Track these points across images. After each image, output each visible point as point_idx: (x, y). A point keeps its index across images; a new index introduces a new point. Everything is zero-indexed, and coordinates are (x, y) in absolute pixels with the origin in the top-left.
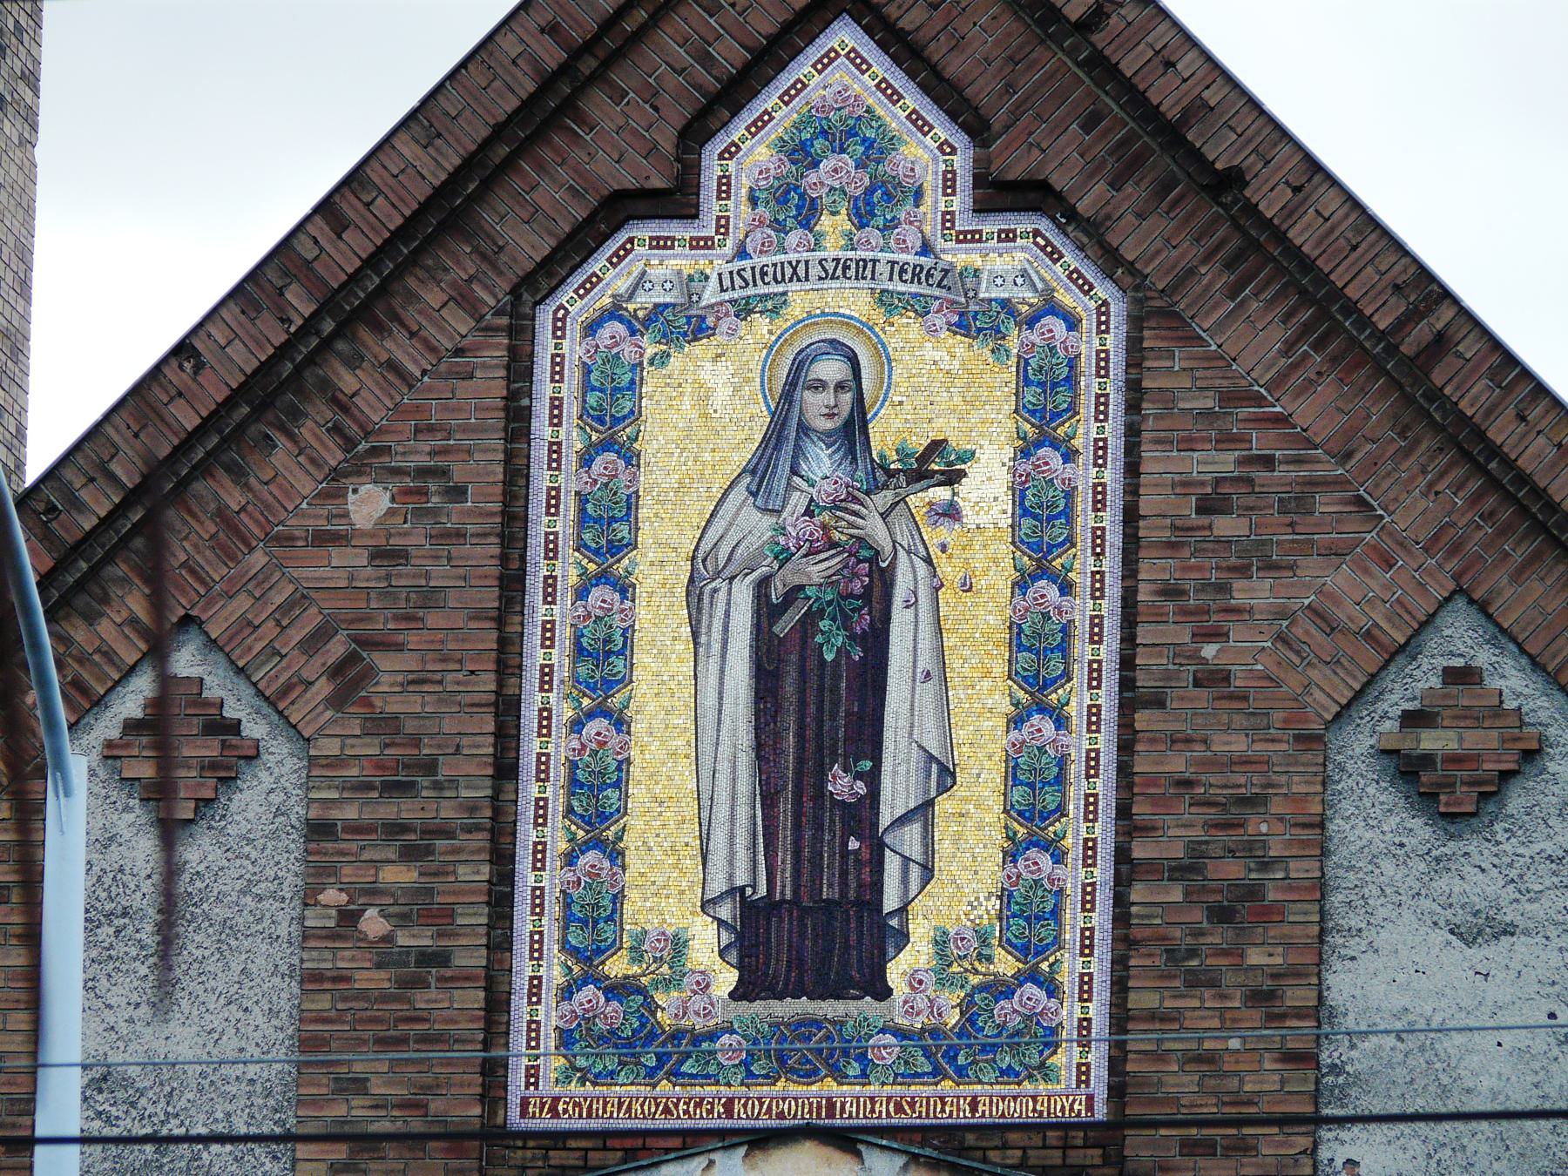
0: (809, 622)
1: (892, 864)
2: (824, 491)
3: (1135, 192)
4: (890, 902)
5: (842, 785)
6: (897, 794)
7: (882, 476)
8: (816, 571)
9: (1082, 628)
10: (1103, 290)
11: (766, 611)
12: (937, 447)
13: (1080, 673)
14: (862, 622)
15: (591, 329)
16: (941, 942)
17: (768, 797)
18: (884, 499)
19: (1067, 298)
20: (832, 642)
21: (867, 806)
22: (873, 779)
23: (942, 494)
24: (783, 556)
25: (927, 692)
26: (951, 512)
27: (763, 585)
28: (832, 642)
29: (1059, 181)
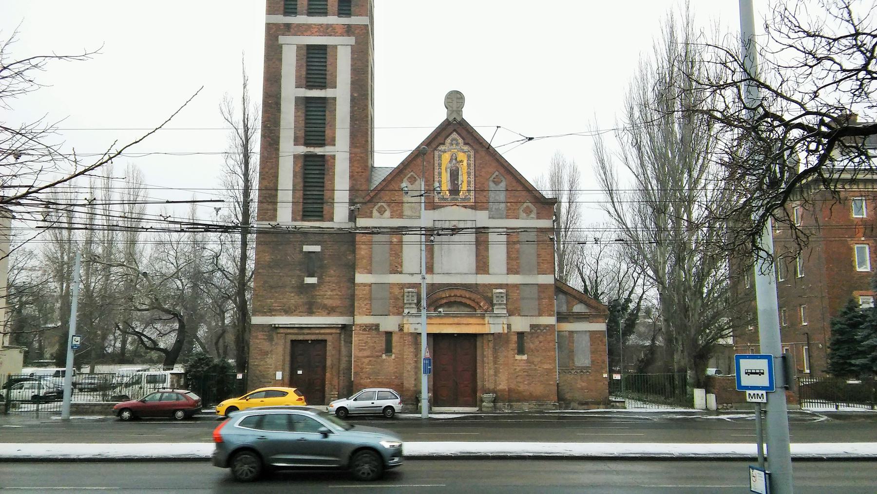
20: (455, 173)
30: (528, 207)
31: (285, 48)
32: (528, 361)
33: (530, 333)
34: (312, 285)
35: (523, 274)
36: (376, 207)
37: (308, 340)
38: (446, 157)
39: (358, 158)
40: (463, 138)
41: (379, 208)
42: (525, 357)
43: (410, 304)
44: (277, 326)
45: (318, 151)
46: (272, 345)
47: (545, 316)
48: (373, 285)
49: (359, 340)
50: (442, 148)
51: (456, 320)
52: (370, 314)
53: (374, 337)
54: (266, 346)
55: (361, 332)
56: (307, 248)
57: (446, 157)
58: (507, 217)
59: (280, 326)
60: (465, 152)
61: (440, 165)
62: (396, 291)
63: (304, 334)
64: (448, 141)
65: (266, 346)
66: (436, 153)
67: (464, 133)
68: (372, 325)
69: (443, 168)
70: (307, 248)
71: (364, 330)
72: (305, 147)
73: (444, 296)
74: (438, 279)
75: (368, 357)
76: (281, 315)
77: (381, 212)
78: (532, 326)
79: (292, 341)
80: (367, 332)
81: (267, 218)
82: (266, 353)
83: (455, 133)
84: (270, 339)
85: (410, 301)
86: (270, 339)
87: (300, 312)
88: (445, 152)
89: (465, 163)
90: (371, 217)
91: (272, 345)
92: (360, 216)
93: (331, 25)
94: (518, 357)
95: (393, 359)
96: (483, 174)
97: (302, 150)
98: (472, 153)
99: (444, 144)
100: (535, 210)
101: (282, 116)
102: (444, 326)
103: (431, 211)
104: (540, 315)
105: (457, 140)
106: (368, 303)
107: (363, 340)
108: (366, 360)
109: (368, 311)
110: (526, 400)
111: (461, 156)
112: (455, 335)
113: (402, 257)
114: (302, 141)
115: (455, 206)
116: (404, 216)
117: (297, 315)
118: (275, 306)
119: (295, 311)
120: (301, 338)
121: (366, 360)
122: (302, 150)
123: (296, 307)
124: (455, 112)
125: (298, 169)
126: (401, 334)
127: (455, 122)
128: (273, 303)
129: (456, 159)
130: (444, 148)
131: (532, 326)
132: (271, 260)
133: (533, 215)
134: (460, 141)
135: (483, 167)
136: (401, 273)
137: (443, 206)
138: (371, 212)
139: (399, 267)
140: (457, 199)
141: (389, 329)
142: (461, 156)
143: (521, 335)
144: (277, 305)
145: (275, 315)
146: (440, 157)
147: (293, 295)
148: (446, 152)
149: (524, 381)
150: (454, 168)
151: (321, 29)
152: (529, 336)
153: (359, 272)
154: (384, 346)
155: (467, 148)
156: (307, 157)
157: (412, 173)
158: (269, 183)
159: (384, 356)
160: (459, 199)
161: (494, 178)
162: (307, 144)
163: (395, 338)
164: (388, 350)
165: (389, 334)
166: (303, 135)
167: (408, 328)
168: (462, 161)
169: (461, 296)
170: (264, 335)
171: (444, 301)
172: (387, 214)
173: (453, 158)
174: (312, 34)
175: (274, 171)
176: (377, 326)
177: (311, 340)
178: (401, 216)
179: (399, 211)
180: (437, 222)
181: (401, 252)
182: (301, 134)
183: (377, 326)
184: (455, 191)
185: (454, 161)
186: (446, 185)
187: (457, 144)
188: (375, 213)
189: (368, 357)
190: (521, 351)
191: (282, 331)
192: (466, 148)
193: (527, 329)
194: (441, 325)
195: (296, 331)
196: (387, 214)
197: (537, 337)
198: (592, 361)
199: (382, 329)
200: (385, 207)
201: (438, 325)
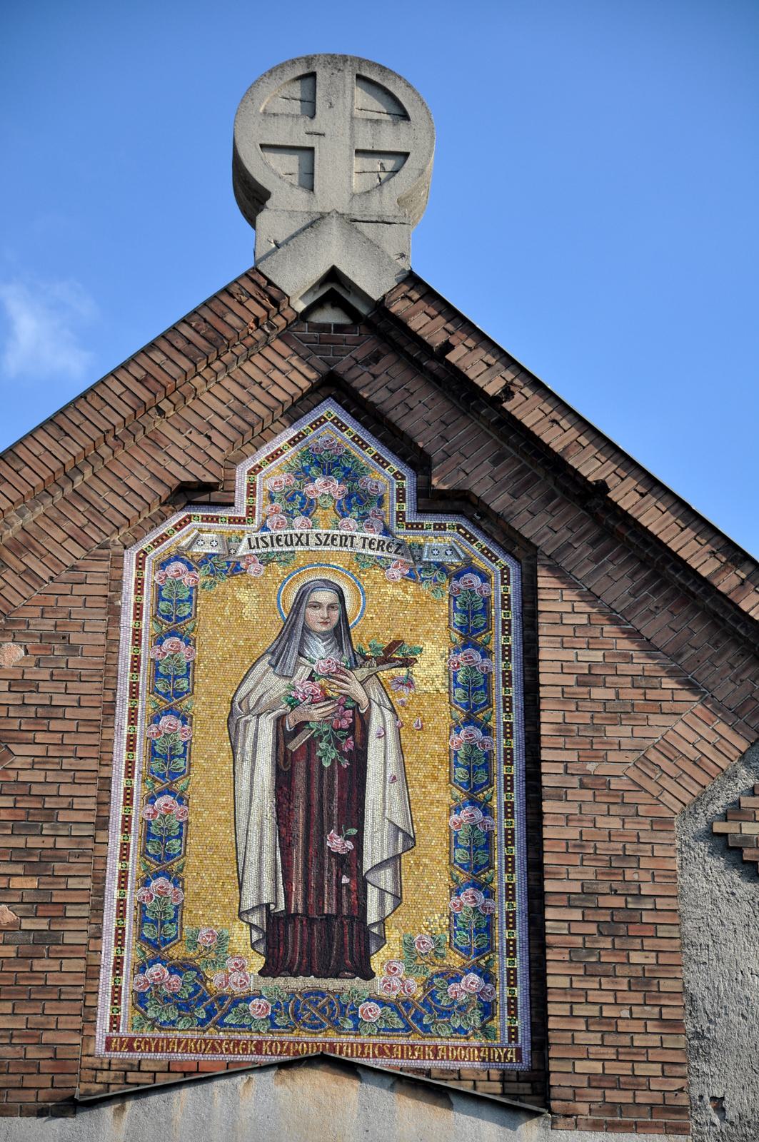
0: (311, 744)
1: (372, 894)
2: (321, 666)
3: (525, 502)
4: (372, 917)
5: (337, 843)
6: (375, 848)
7: (358, 659)
8: (316, 713)
9: (499, 755)
10: (504, 561)
11: (282, 735)
12: (396, 644)
13: (499, 783)
14: (348, 745)
15: (163, 565)
16: (408, 945)
17: (285, 845)
18: (361, 673)
19: (481, 563)
20: (327, 756)
21: (351, 861)
22: (358, 840)
23: (403, 672)
24: (294, 703)
25: (394, 790)
26: (408, 683)
27: (280, 720)
28: (327, 756)
29: (479, 491)
40: (419, 462)
83: (329, 409)
96: (616, 767)
105: (351, 474)
115: (316, 1082)
124: (333, 230)
127: (329, 316)
129: (340, 633)
135: (620, 712)
137: (196, 1077)
148: (236, 569)
155: (448, 539)
160: (372, 1012)
161: (735, 811)
185: (320, 651)
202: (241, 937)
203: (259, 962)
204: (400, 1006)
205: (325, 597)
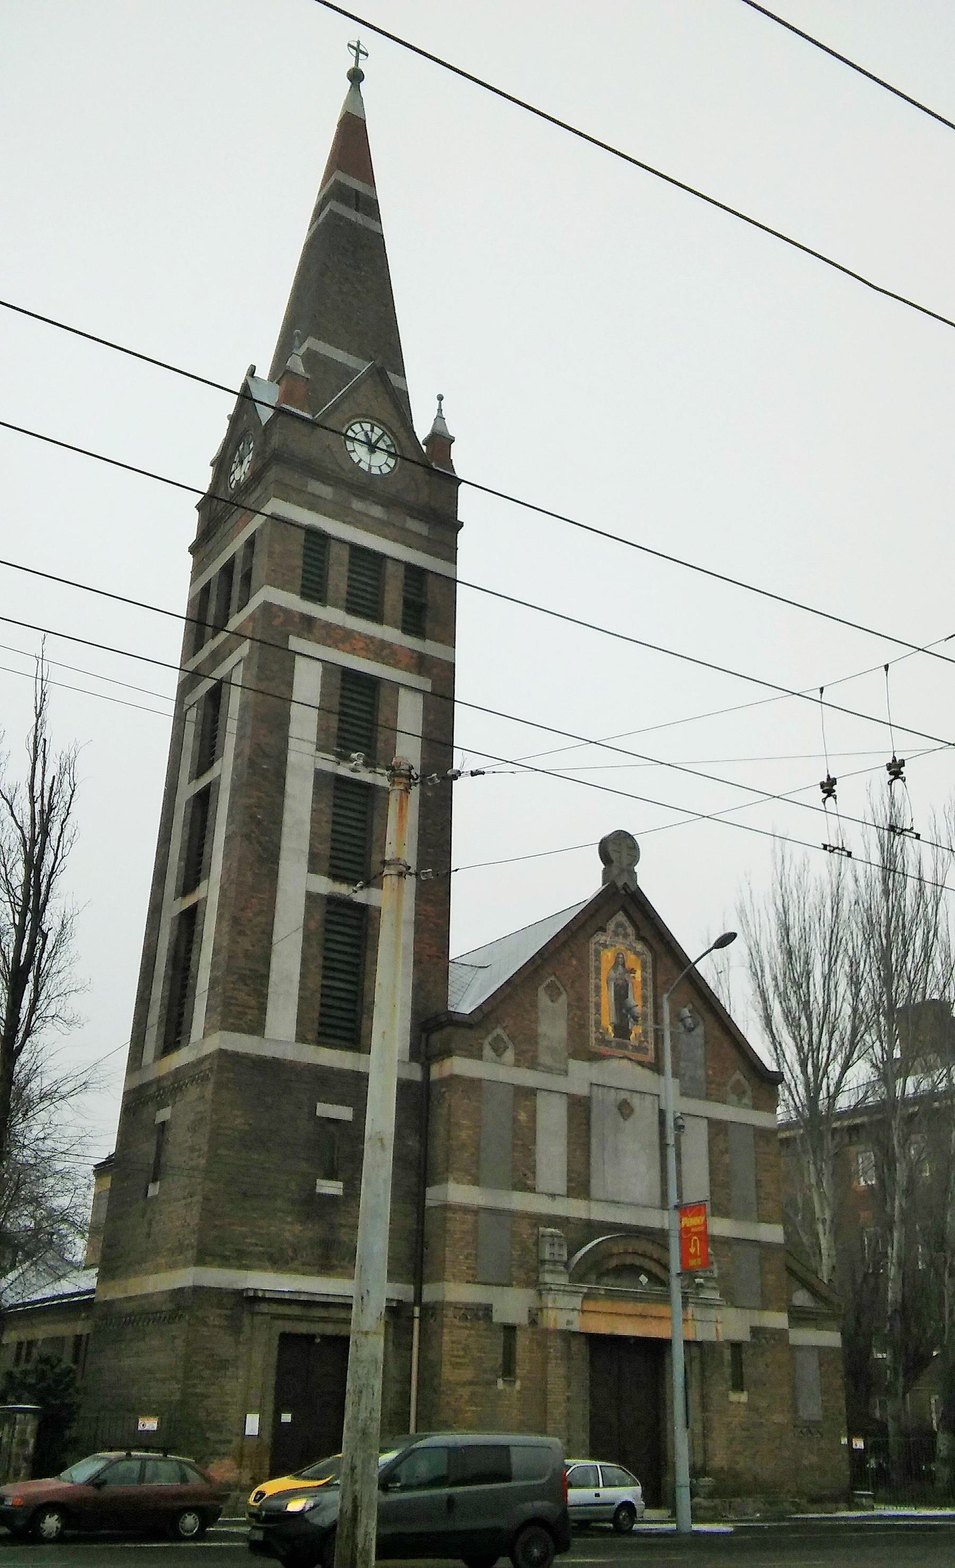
11: (616, 986)
23: (632, 975)
26: (634, 978)
30: (738, 1081)
31: (300, 662)
32: (750, 1406)
33: (753, 1346)
34: (332, 1199)
35: (737, 1219)
36: (490, 1038)
37: (313, 1337)
38: (608, 956)
39: (431, 925)
41: (495, 1039)
42: (743, 1397)
43: (555, 1262)
44: (260, 1294)
45: (360, 897)
46: (237, 1343)
47: (773, 1310)
48: (482, 1215)
49: (453, 1342)
50: (601, 938)
51: (640, 1307)
52: (473, 1280)
53: (481, 1336)
54: (224, 1346)
55: (457, 1322)
56: (325, 1110)
57: (608, 956)
58: (708, 1097)
59: (268, 1295)
60: (637, 954)
61: (598, 970)
62: (525, 1230)
63: (311, 1320)
64: (611, 926)
65: (224, 1346)
66: (592, 946)
67: (637, 916)
68: (479, 1306)
69: (604, 975)
70: (325, 1110)
71: (464, 1318)
72: (330, 881)
73: (615, 1250)
74: (599, 1213)
75: (471, 1383)
76: (263, 1269)
77: (498, 1050)
78: (756, 1331)
79: (285, 1338)
80: (469, 1325)
81: (245, 1026)
82: (223, 1365)
84: (235, 1327)
85: (557, 1258)
86: (235, 1327)
87: (303, 1264)
88: (605, 946)
89: (638, 974)
90: (480, 1057)
91: (237, 1343)
92: (457, 1052)
93: (391, 645)
94: (734, 1397)
95: (519, 1392)
97: (324, 885)
98: (649, 958)
99: (603, 929)
100: (749, 1093)
101: (288, 802)
102: (618, 1318)
103: (586, 1064)
104: (764, 1307)
105: (625, 929)
106: (470, 1254)
107: (460, 1343)
108: (465, 1392)
109: (471, 1272)
110: (749, 1493)
111: (632, 960)
112: (632, 1341)
113: (534, 1154)
114: (326, 866)
115: (625, 1061)
116: (539, 1064)
117: (296, 1271)
118: (251, 1244)
119: (292, 1259)
120: (303, 1328)
121: (465, 1392)
122: (324, 885)
123: (295, 1251)
125: (313, 925)
126: (533, 1333)
128: (245, 1237)
129: (623, 965)
130: (604, 938)
131: (756, 1331)
132: (246, 1127)
133: (746, 1100)
134: (630, 930)
136: (532, 1190)
138: (481, 1049)
139: (529, 1175)
140: (625, 1047)
141: (511, 1320)
142: (632, 960)
143: (736, 1346)
144: (254, 1241)
145: (247, 1268)
146: (597, 954)
147: (289, 1219)
149: (744, 1450)
150: (620, 982)
151: (371, 646)
152: (751, 1352)
153: (454, 1179)
154: (500, 1361)
156: (332, 900)
157: (553, 978)
158: (253, 946)
159: (500, 1381)
162: (335, 877)
163: (522, 1342)
164: (508, 1369)
165: (510, 1330)
166: (328, 852)
167: (555, 1320)
168: (633, 971)
169: (644, 1255)
170: (220, 1316)
171: (614, 1262)
172: (509, 1055)
173: (619, 962)
174: (353, 651)
175: (264, 920)
176: (488, 1309)
177: (324, 1337)
178: (533, 1065)
179: (531, 1054)
180: (595, 1088)
181: (534, 1142)
182: (324, 849)
183: (488, 1309)
184: (622, 1031)
185: (620, 968)
186: (608, 1018)
187: (626, 936)
188: (488, 1051)
189: (471, 1383)
190: (738, 1386)
191: (264, 1308)
192: (639, 947)
193: (743, 1335)
194: (614, 1317)
195: (296, 1311)
196: (509, 1055)
197: (762, 1354)
198: (825, 1409)
199: (496, 1318)
200: (506, 1038)
201: (608, 1318)
202: (610, 1029)
203: (613, 1035)
204: (634, 1047)
205: (621, 956)
